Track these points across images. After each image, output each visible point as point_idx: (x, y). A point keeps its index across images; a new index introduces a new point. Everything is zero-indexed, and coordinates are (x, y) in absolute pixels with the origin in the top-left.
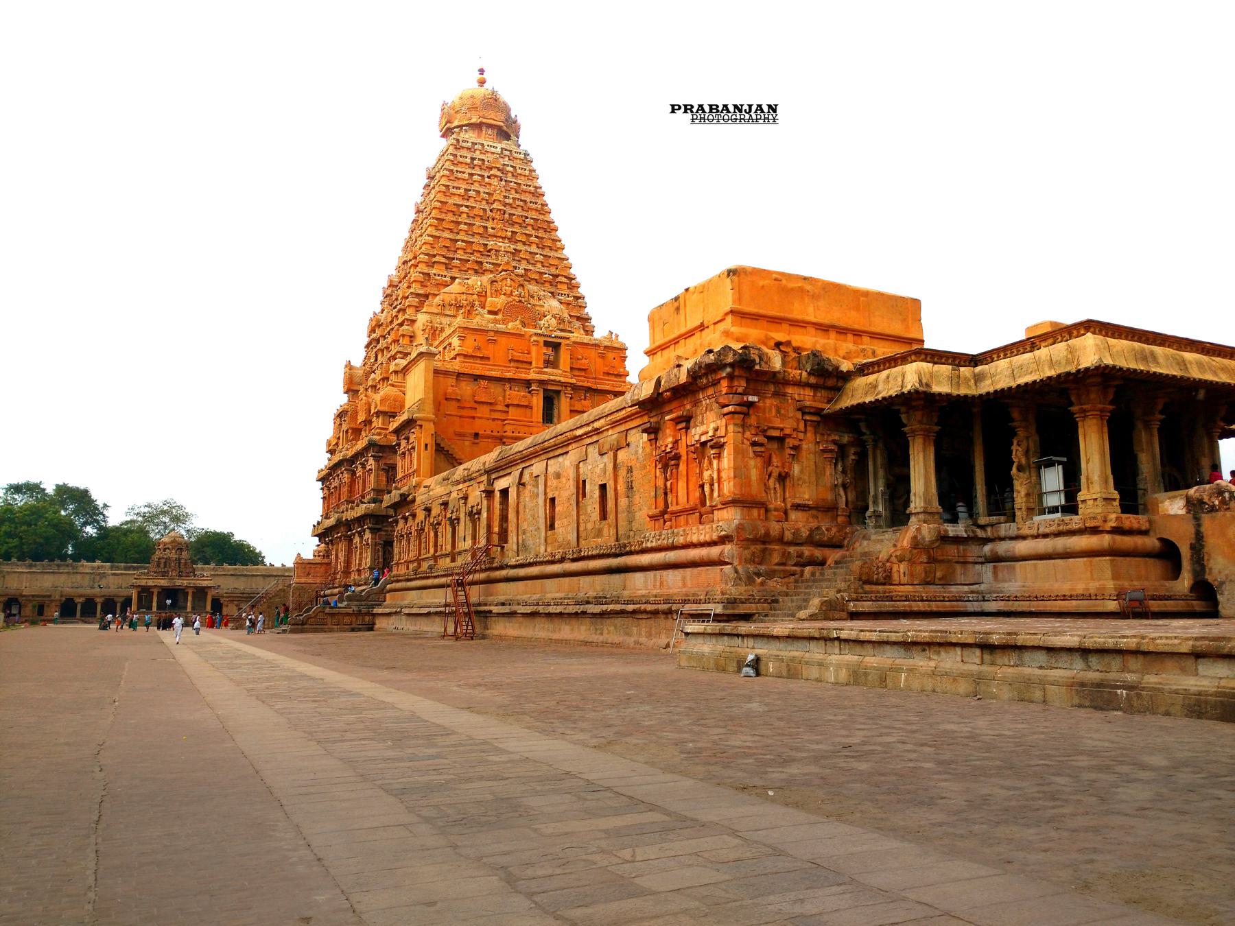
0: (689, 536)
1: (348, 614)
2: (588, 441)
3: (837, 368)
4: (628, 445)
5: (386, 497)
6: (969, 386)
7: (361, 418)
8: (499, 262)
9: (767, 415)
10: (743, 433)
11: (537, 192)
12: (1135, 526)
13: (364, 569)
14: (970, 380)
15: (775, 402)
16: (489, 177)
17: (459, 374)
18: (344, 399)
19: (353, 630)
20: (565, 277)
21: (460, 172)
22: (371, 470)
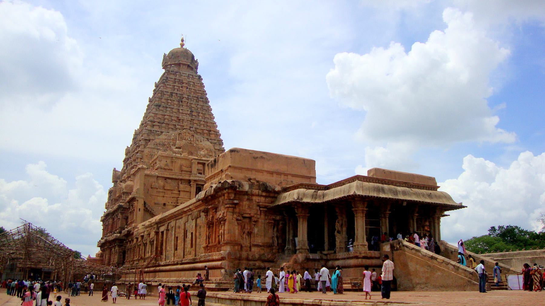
0: (213, 257)
2: (189, 213)
3: (274, 190)
4: (200, 216)
5: (123, 231)
7: (117, 195)
8: (183, 125)
9: (244, 208)
11: (203, 94)
12: (373, 255)
16: (182, 87)
17: (158, 176)
18: (112, 185)
20: (214, 131)
21: (169, 85)
22: (119, 218)
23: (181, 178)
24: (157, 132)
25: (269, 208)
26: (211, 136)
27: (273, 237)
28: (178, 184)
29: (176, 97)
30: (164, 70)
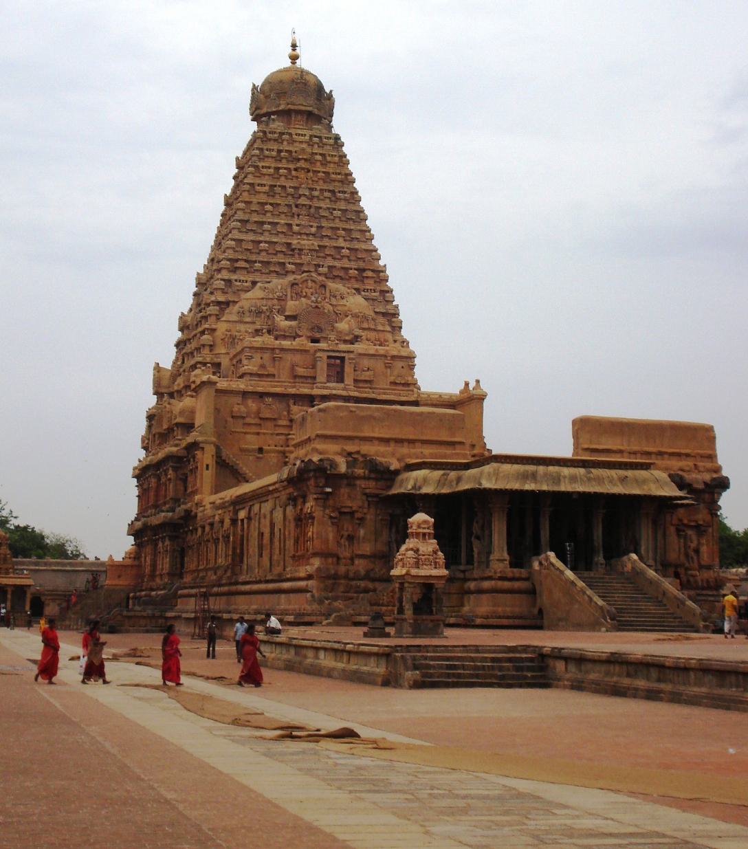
1: (144, 617)
2: (276, 495)
3: (389, 468)
6: (452, 485)
7: (165, 427)
10: (324, 511)
11: (347, 179)
12: (517, 575)
13: (164, 574)
14: (452, 481)
15: (347, 490)
16: (296, 170)
18: (153, 400)
19: (147, 631)
21: (266, 167)
22: (170, 479)
23: (293, 393)
24: (245, 284)
25: (380, 498)
26: (366, 281)
27: (389, 542)
28: (289, 406)
29: (284, 195)
30: (256, 122)
